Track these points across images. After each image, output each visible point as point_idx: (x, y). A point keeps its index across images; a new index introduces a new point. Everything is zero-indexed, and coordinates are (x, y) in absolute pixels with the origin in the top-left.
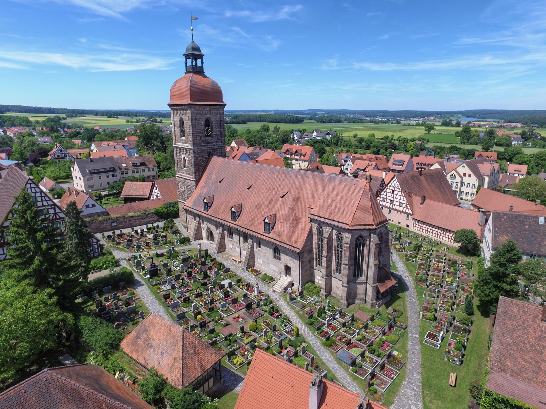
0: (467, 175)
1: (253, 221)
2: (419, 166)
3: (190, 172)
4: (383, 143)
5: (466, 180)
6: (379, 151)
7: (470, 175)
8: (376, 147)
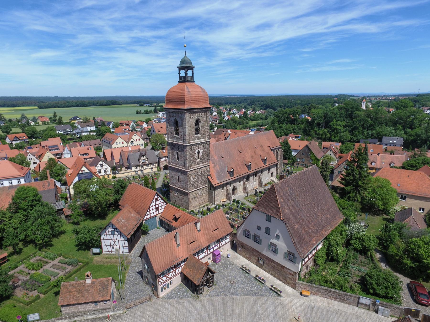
0: (138, 140)
3: (204, 161)
7: (139, 140)
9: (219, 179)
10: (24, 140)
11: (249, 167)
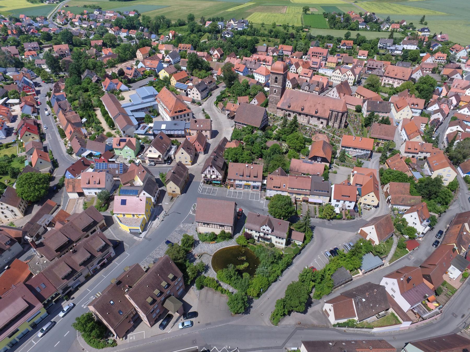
1: (310, 111)
2: (313, 54)
4: (286, 34)
5: (350, 77)
6: (285, 41)
8: (284, 38)
9: (281, 105)
10: (350, 46)
11: (303, 110)
